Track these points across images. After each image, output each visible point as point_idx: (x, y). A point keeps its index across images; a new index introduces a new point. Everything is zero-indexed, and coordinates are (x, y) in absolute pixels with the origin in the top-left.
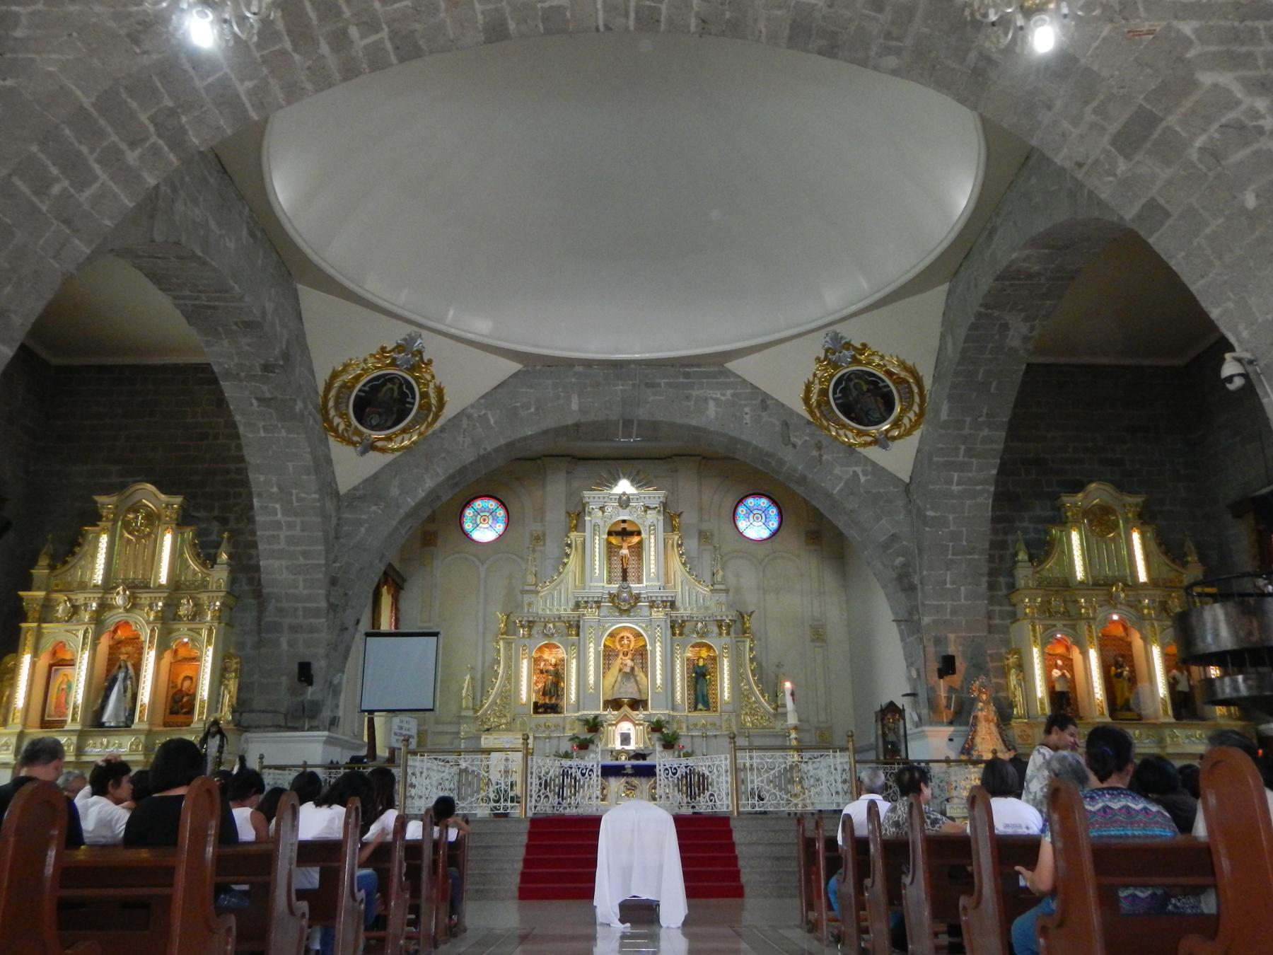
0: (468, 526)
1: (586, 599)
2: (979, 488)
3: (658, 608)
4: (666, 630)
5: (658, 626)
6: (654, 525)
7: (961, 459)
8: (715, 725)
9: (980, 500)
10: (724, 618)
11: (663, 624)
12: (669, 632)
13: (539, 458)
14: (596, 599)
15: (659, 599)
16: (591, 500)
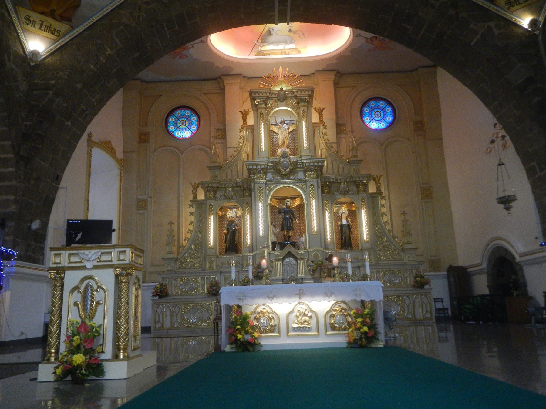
0: (171, 128)
1: (255, 167)
3: (311, 171)
4: (318, 187)
5: (312, 185)
6: (305, 112)
8: (358, 258)
10: (361, 179)
11: (315, 183)
12: (320, 190)
13: (220, 78)
14: (263, 166)
15: (312, 164)
16: (257, 95)
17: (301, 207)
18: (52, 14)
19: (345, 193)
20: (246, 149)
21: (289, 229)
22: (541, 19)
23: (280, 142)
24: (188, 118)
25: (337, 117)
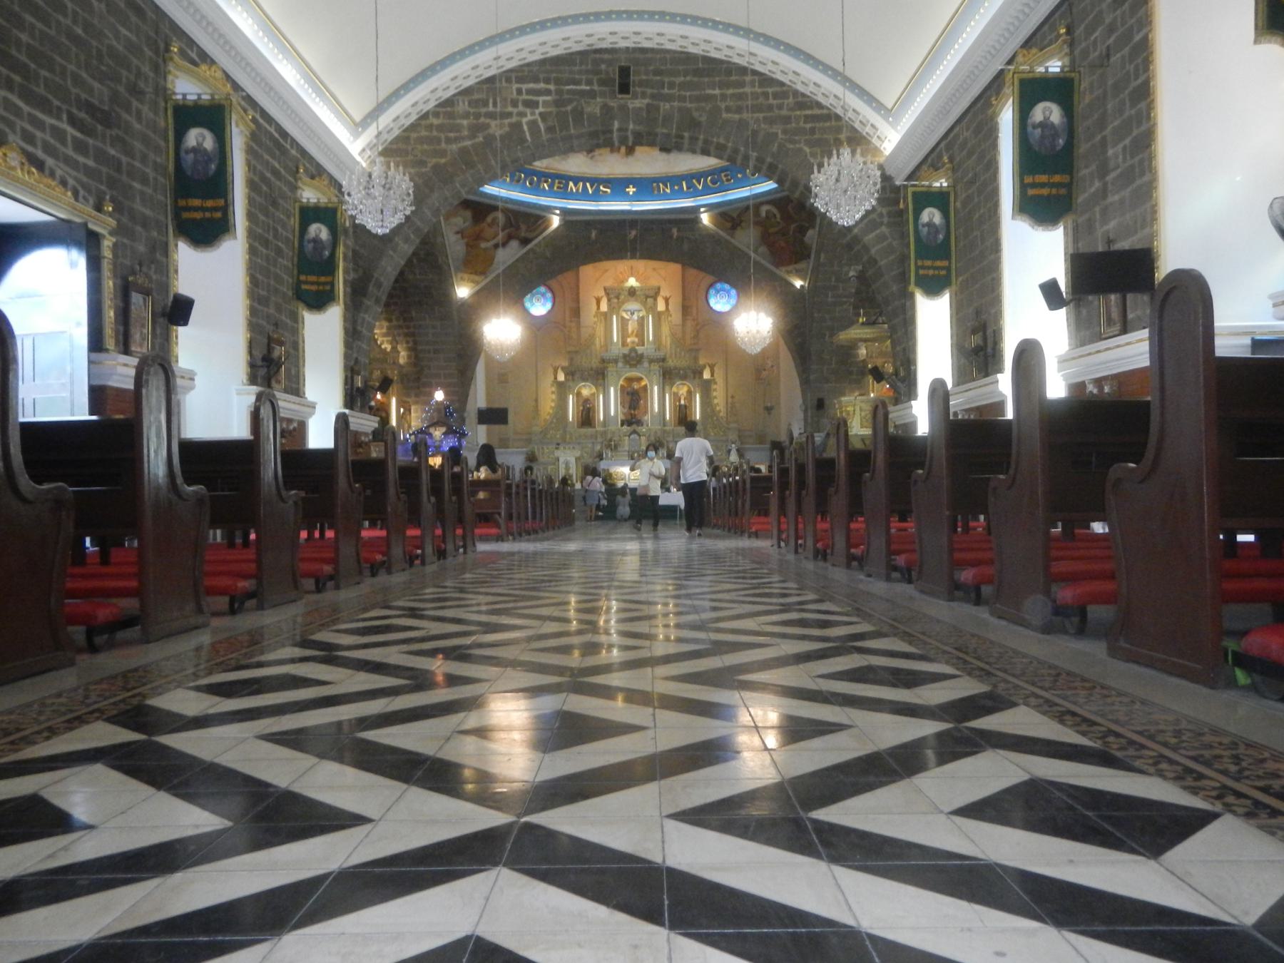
0: (528, 305)
2: (845, 300)
7: (833, 283)
9: (845, 307)
11: (657, 373)
17: (645, 388)
18: (476, 273)
19: (684, 378)
20: (600, 331)
21: (634, 409)
22: (807, 285)
23: (630, 330)
24: (543, 295)
25: (684, 298)
